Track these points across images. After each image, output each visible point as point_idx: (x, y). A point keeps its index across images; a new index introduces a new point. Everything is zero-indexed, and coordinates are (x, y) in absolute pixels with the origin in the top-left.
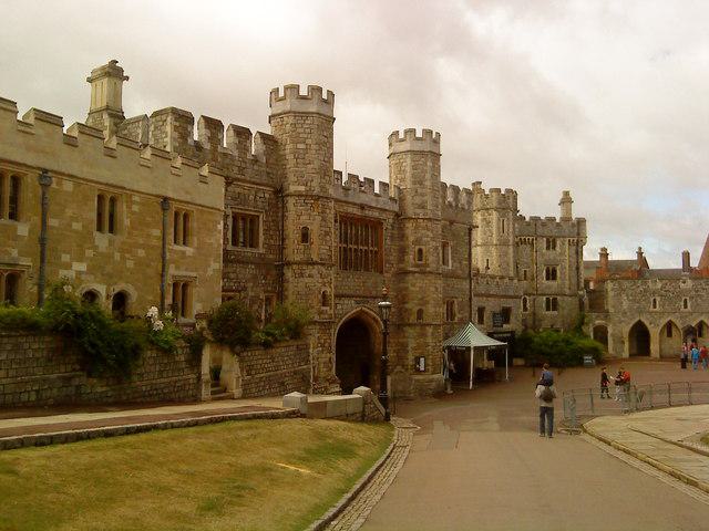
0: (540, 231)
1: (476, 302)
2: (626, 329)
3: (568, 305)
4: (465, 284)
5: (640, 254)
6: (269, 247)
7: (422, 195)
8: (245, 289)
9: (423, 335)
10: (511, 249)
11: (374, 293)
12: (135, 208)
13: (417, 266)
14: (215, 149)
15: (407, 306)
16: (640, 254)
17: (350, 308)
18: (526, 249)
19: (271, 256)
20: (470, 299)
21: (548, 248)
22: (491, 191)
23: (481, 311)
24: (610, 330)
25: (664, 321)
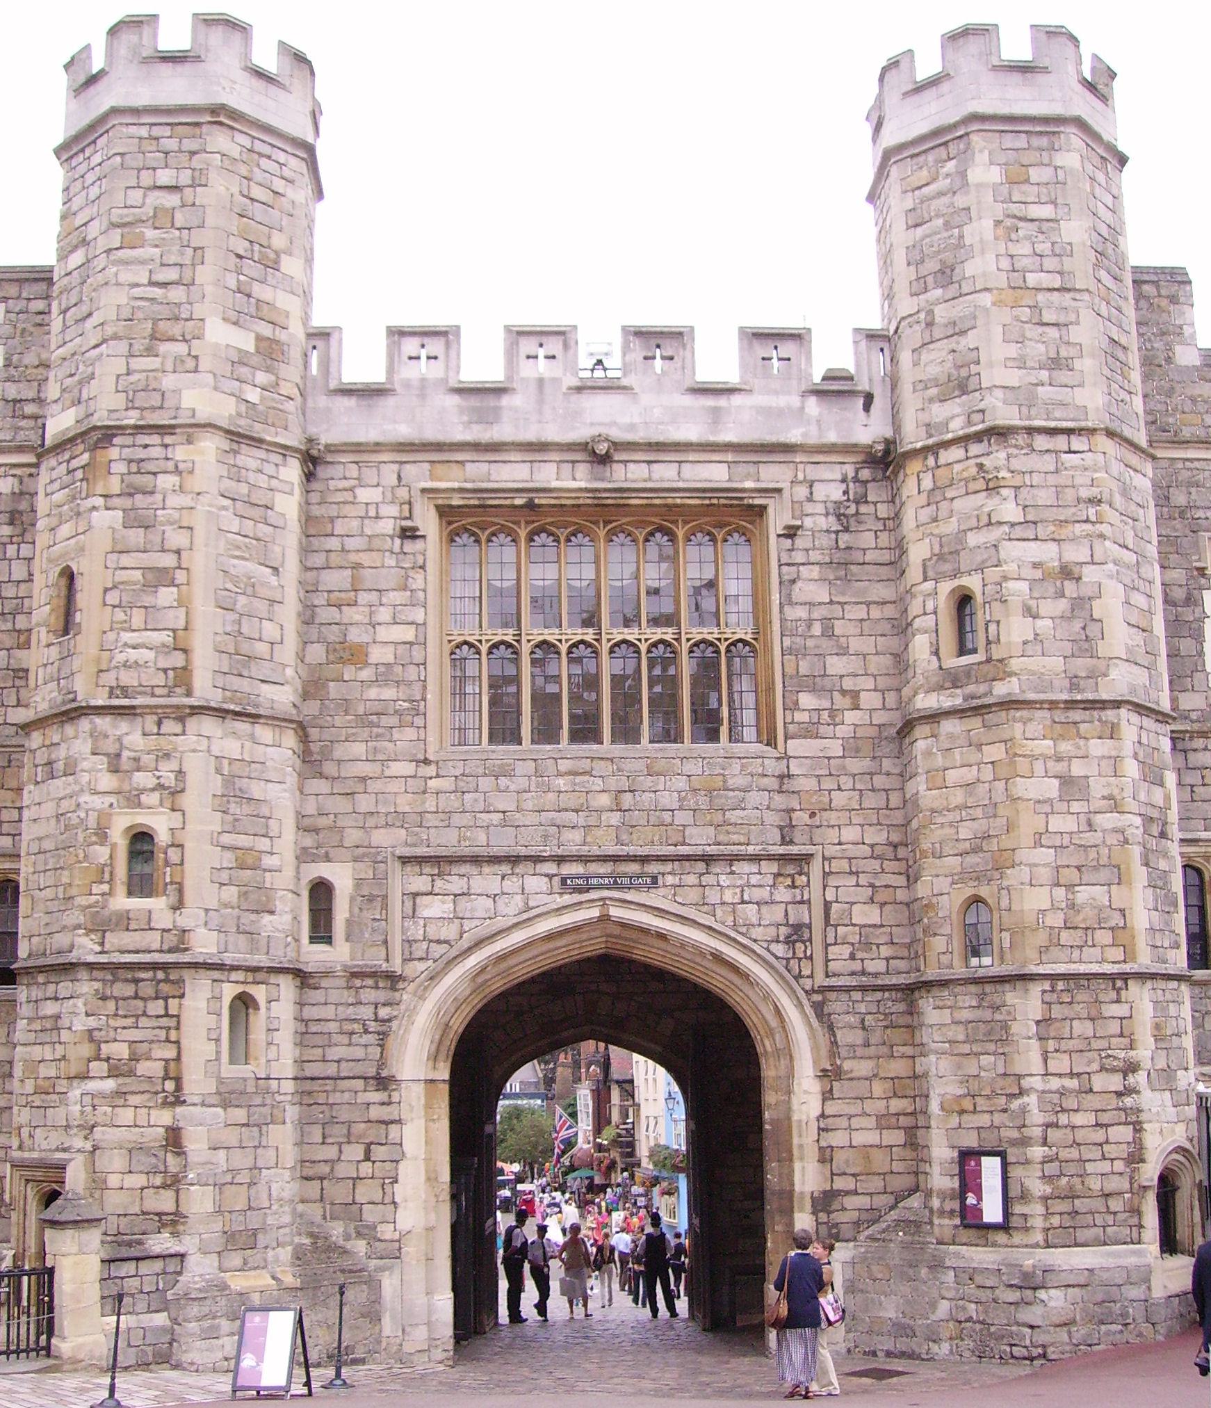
11: (700, 839)
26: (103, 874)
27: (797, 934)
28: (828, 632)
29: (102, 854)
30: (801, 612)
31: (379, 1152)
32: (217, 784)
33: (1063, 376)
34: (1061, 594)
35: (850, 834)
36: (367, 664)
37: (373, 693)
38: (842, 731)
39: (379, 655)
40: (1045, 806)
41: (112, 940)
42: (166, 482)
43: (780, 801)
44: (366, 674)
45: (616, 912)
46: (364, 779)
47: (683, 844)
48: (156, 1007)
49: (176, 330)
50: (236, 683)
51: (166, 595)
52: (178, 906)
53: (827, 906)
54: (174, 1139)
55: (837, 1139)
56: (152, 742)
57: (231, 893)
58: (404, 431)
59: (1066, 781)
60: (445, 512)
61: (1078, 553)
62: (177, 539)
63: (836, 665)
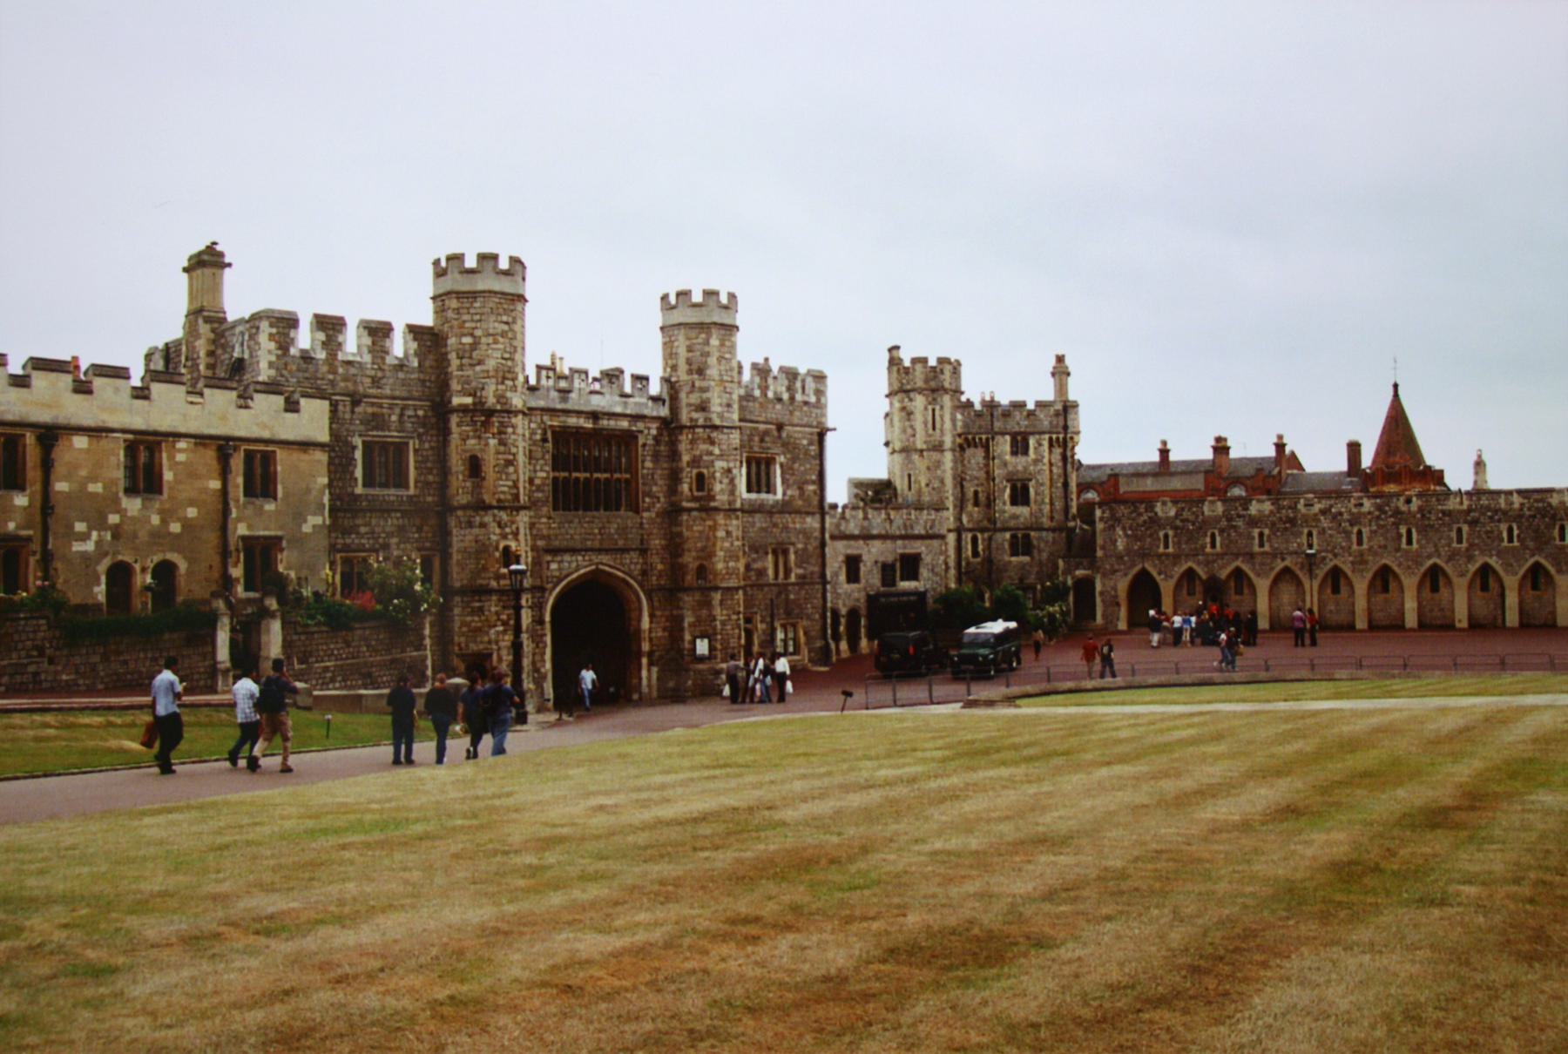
0: (998, 425)
1: (836, 552)
2: (1123, 585)
3: (1044, 541)
4: (812, 522)
5: (1280, 447)
6: (423, 485)
7: (704, 390)
8: (386, 547)
9: (707, 604)
10: (948, 457)
11: (621, 543)
12: (180, 457)
13: (694, 499)
14: (332, 356)
15: (680, 560)
16: (1280, 447)
17: (575, 567)
18: (976, 456)
19: (429, 499)
20: (823, 545)
21: (1014, 453)
22: (915, 361)
23: (853, 564)
24: (1098, 587)
25: (1179, 570)
27: (644, 573)
40: (723, 540)
42: (510, 430)
45: (601, 567)
49: (509, 376)
51: (511, 469)
58: (542, 403)
60: (554, 433)
61: (731, 465)
62: (514, 450)
63: (655, 489)
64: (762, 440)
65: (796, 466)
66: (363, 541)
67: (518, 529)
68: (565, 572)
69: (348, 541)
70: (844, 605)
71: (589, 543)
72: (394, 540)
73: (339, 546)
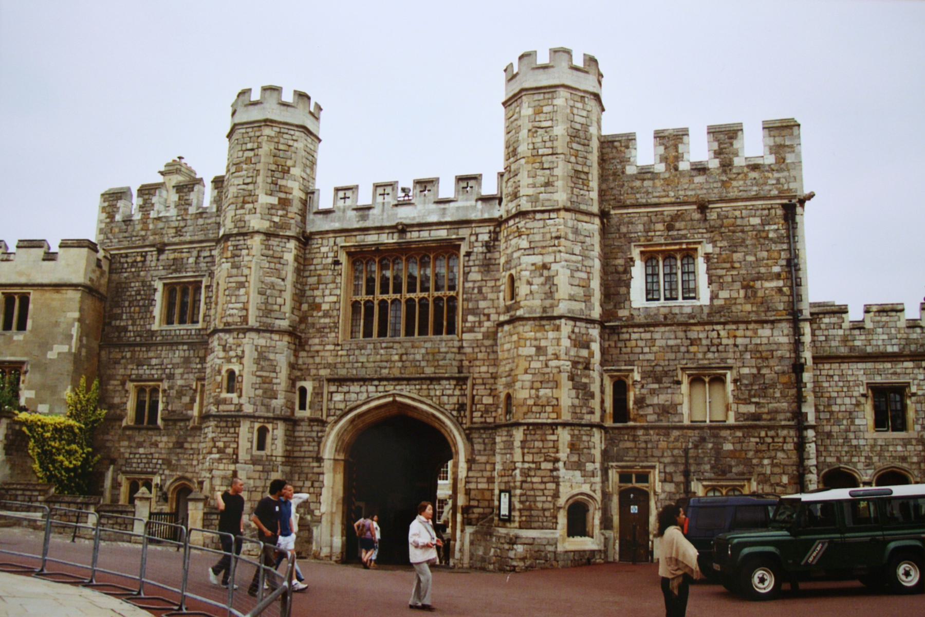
4: (781, 336)
8: (171, 377)
11: (429, 371)
20: (798, 368)
26: (219, 386)
27: (461, 407)
28: (480, 291)
29: (219, 378)
30: (470, 285)
31: (316, 484)
32: (256, 355)
33: (550, 189)
34: (542, 275)
35: (484, 369)
36: (320, 310)
37: (322, 321)
38: (483, 330)
39: (325, 307)
40: (529, 358)
41: (221, 407)
42: (244, 252)
43: (458, 357)
44: (321, 314)
45: (398, 399)
46: (318, 352)
47: (423, 373)
48: (232, 430)
49: (250, 199)
50: (264, 319)
51: (242, 291)
52: (240, 396)
53: (473, 397)
54: (235, 474)
55: (472, 486)
56: (235, 341)
57: (260, 392)
58: (337, 225)
59: (539, 349)
60: (349, 254)
61: (549, 259)
62: (246, 271)
63: (482, 304)
64: (670, 227)
65: (737, 256)
66: (153, 372)
67: (243, 352)
68: (351, 405)
69: (141, 372)
70: (868, 465)
71: (385, 372)
72: (178, 371)
73: (134, 377)
